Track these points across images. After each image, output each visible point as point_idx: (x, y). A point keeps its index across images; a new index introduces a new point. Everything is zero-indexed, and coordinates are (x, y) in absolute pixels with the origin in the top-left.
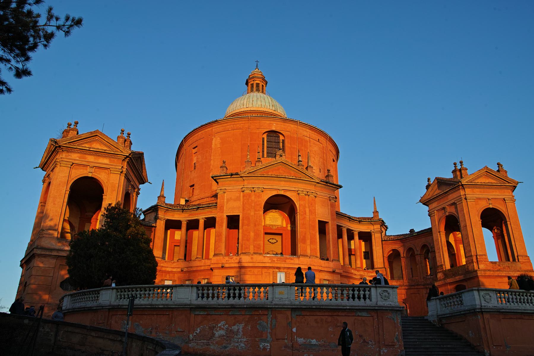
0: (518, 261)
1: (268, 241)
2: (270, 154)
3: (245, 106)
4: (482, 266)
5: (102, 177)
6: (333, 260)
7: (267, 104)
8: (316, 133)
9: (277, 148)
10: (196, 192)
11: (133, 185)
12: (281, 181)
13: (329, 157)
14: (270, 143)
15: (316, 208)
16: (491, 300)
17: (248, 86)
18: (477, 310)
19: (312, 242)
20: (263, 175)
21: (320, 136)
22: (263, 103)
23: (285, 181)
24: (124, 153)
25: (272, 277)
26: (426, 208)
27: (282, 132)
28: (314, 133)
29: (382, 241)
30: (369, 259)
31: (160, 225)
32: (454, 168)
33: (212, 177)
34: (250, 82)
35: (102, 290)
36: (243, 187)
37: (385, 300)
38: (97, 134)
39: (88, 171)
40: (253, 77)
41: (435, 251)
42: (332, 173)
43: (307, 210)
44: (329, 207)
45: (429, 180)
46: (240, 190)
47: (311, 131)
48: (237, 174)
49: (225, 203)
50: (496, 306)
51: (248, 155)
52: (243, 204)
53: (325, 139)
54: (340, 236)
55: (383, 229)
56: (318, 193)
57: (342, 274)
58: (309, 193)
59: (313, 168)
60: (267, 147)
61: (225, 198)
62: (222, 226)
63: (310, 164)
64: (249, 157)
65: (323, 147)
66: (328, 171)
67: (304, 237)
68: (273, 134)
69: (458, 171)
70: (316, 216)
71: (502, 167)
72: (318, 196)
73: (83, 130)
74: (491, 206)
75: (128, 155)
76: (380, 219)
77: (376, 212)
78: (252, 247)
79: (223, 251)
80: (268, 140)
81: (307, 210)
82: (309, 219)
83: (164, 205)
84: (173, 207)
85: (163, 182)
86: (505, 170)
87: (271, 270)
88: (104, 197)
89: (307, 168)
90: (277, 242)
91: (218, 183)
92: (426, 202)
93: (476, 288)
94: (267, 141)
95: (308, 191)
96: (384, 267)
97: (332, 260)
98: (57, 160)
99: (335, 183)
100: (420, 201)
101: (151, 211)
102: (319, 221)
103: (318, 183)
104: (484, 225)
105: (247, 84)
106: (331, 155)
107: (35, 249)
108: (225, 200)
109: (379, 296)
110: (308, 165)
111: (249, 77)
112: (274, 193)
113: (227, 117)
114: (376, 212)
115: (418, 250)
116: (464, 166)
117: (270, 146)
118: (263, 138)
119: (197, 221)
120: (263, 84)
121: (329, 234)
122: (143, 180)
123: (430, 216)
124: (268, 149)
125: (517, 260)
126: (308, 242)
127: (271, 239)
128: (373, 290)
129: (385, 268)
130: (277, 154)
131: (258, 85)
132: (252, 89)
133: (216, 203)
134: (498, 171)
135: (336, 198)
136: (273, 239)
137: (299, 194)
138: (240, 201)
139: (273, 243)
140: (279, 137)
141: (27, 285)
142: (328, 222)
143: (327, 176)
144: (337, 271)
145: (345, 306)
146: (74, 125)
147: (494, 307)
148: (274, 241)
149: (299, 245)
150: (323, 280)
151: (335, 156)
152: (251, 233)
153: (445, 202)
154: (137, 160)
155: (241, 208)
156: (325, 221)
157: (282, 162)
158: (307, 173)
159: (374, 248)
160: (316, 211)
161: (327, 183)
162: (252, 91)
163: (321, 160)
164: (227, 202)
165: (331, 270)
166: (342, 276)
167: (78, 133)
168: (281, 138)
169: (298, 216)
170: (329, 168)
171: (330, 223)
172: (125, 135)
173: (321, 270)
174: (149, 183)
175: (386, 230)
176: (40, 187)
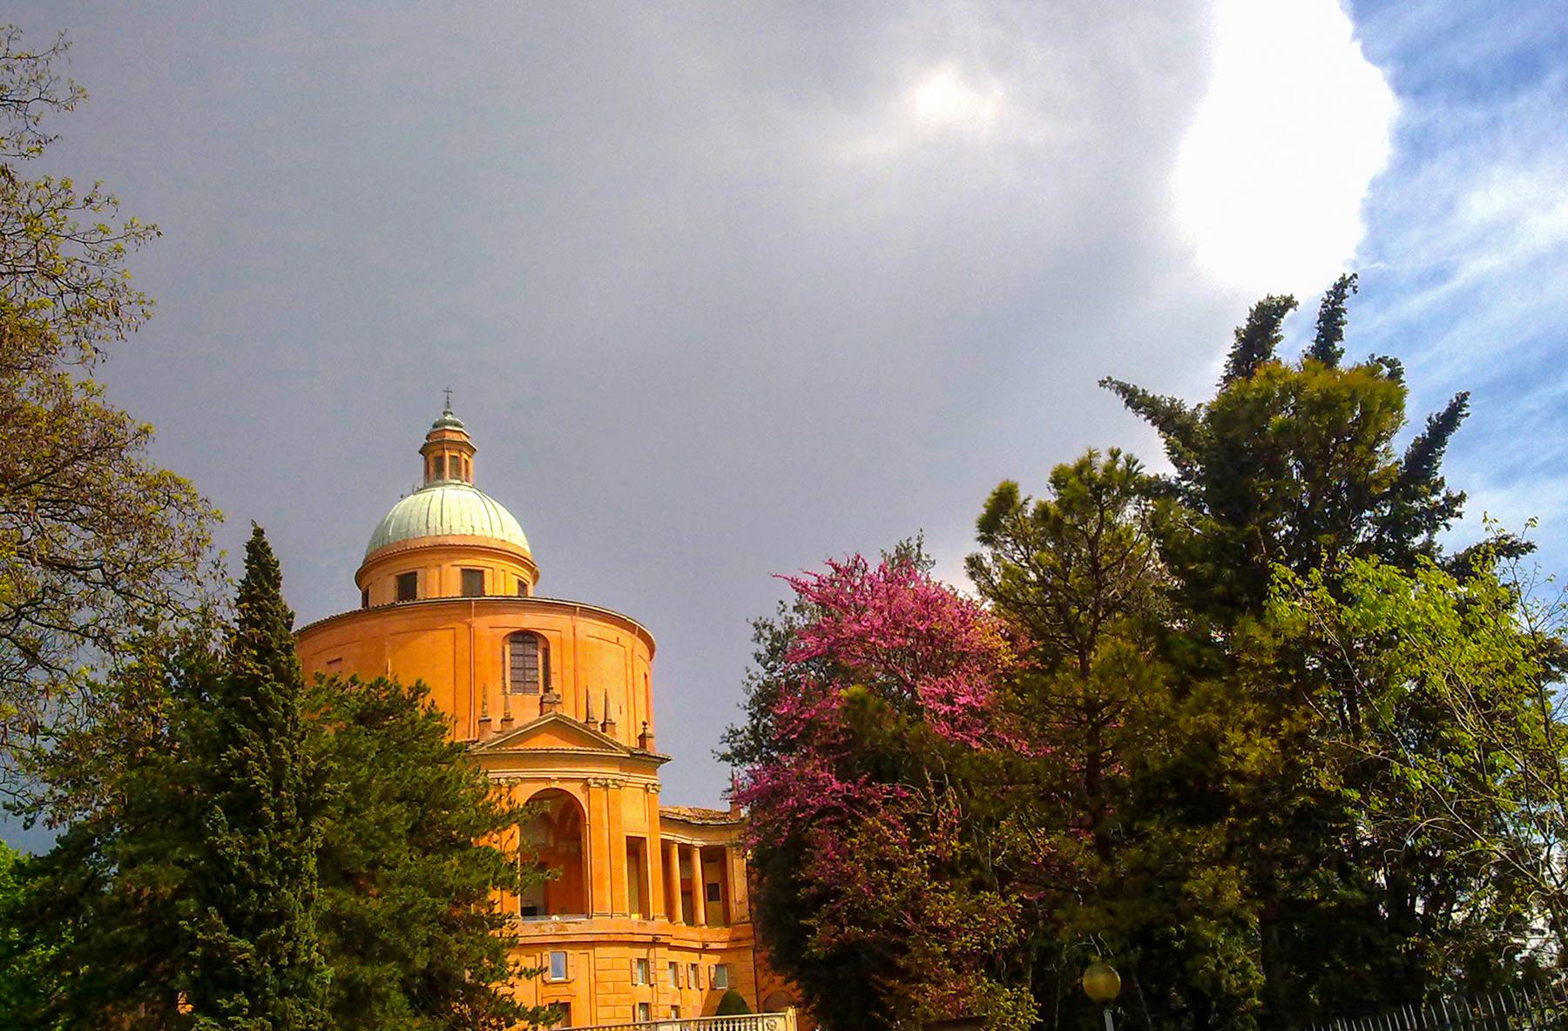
2: (517, 685)
7: (487, 528)
8: (612, 626)
28: (607, 625)
43: (605, 815)
63: (613, 716)
67: (601, 875)
68: (526, 638)
89: (603, 725)
118: (504, 648)
120: (467, 458)
143: (643, 738)
144: (663, 940)
156: (638, 835)
163: (623, 684)
165: (649, 939)
166: (672, 948)
168: (541, 645)
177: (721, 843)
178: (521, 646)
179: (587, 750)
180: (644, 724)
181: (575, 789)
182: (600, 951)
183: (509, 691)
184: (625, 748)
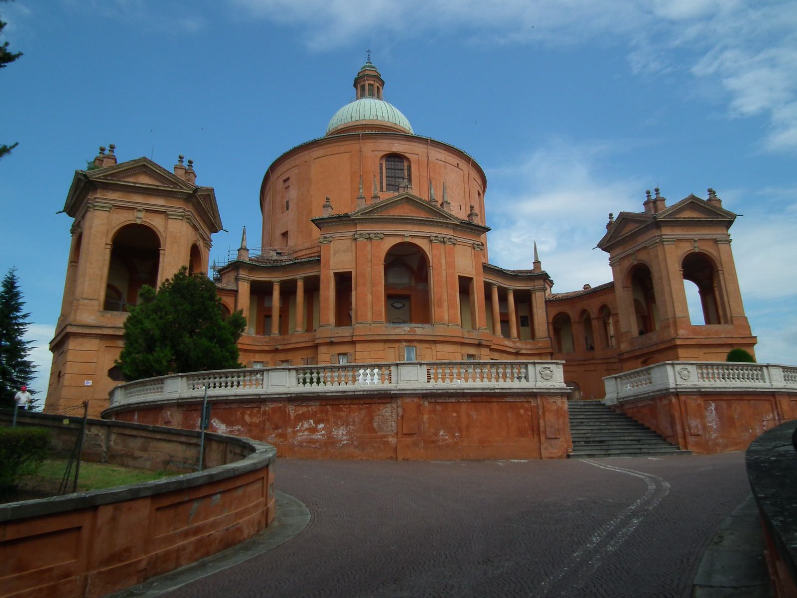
0: (732, 323)
1: (392, 305)
2: (391, 187)
3: (354, 119)
4: (682, 332)
5: (156, 222)
6: (479, 329)
9: (401, 178)
10: (291, 242)
11: (202, 235)
12: (407, 223)
13: (472, 188)
14: (390, 171)
15: (456, 260)
16: (689, 377)
17: (357, 89)
18: (671, 390)
19: (451, 306)
20: (382, 216)
21: (458, 158)
22: (379, 114)
23: (412, 224)
24: (184, 190)
25: (397, 353)
26: (607, 255)
27: (406, 155)
28: (450, 154)
29: (546, 302)
30: (528, 326)
31: (244, 289)
32: (646, 199)
33: (313, 221)
34: (359, 83)
35: (167, 378)
36: (355, 233)
37: (546, 380)
38: (145, 164)
39: (136, 216)
40: (364, 76)
41: (617, 314)
42: (476, 210)
43: (443, 261)
44: (473, 257)
45: (611, 215)
46: (351, 237)
47: (446, 153)
48: (346, 216)
49: (332, 256)
50: (696, 385)
51: (360, 188)
52: (356, 256)
53: (467, 164)
54: (488, 297)
55: (547, 286)
56: (458, 239)
57: (492, 347)
58: (445, 239)
59: (451, 204)
60: (387, 177)
61: (332, 249)
62: (329, 288)
64: (361, 191)
65: (464, 175)
66: (472, 207)
68: (394, 157)
69: (653, 203)
70: (455, 270)
71: (715, 194)
72: (458, 243)
73: (124, 156)
74: (697, 250)
75: (192, 192)
76: (543, 272)
77: (537, 263)
78: (369, 314)
79: (332, 319)
80: (387, 167)
81: (443, 261)
82: (445, 275)
83: (248, 260)
84: (260, 263)
85: (244, 229)
86: (719, 198)
87: (396, 345)
88: (161, 252)
89: (442, 205)
90: (404, 306)
91: (320, 228)
92: (605, 245)
93: (670, 362)
94: (386, 169)
95: (444, 236)
96: (549, 336)
97: (477, 328)
98: (90, 201)
99: (480, 224)
100: (599, 246)
101: (229, 269)
102: (460, 277)
103: (457, 225)
104: (687, 276)
105: (355, 85)
106: (476, 186)
107: (68, 327)
108: (332, 252)
109: (539, 376)
110: (443, 200)
111: (358, 75)
112: (398, 240)
113: (330, 135)
114: (537, 263)
115: (594, 312)
116: (661, 195)
117: (390, 175)
118: (381, 164)
119: (294, 282)
120: (379, 86)
121: (473, 293)
122: (215, 227)
123: (611, 266)
124: (388, 179)
125: (730, 322)
126: (445, 304)
127: (395, 302)
128: (530, 367)
129: (551, 338)
130: (400, 186)
131: (372, 85)
132: (362, 94)
133: (319, 256)
134: (709, 200)
135: (483, 245)
136: (398, 303)
137: (431, 241)
138: (352, 251)
139: (398, 308)
140: (403, 162)
141: (61, 375)
142: (472, 278)
143: (470, 216)
144: (484, 343)
145: (494, 389)
146: (110, 150)
147: (694, 385)
148: (399, 305)
149: (433, 310)
150: (466, 355)
151: (481, 187)
152: (368, 294)
153: (632, 247)
154: (204, 199)
155: (354, 263)
157: (407, 197)
158: (443, 212)
159: (535, 310)
160: (456, 263)
161: (469, 224)
162: (363, 96)
164: (334, 255)
165: (476, 342)
166: (492, 350)
167: (116, 162)
168: (406, 164)
169: (431, 270)
170: (473, 204)
171: (474, 279)
172: (185, 164)
173: (463, 342)
174: (225, 230)
175: (551, 287)
176: (68, 240)
177: (528, 288)
178: (393, 163)
179: (430, 217)
180: (472, 207)
181: (423, 244)
182: (440, 347)
183: (385, 189)
184: (456, 218)
